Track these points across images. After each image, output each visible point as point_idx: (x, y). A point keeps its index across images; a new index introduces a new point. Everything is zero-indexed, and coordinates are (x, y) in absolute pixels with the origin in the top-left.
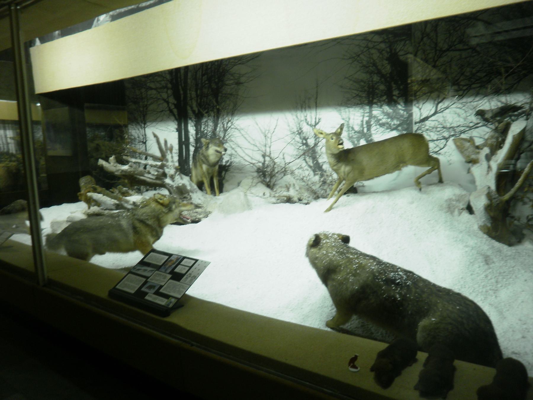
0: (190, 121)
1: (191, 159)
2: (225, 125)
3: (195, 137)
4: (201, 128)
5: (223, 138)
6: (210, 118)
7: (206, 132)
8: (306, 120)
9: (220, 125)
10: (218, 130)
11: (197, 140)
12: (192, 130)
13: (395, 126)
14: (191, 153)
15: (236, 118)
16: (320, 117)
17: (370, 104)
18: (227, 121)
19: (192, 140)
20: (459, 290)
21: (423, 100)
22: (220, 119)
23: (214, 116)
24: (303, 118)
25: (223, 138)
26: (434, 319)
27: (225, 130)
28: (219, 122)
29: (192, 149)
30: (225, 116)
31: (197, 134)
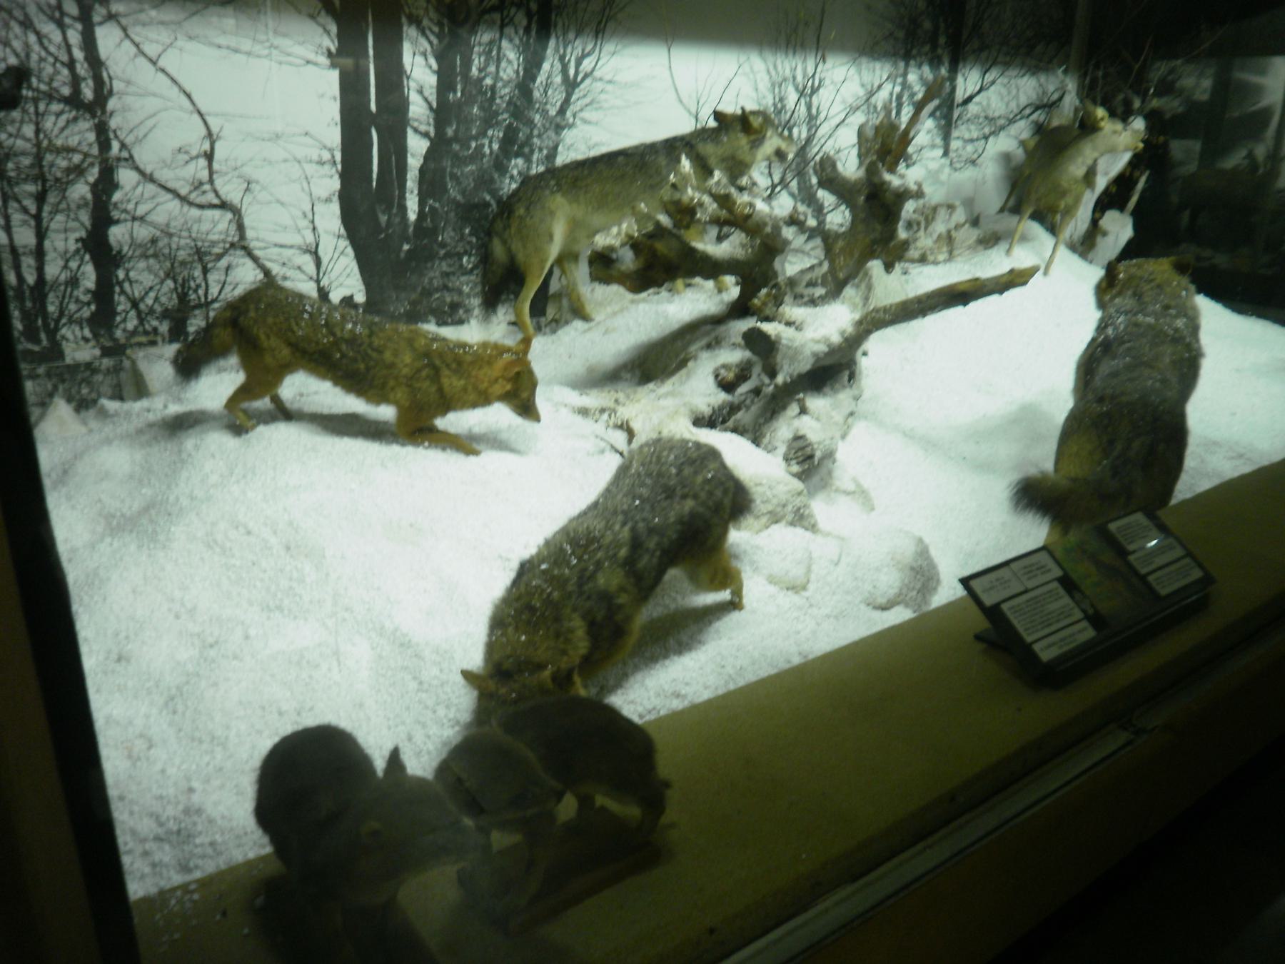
0: (410, 32)
1: (412, 182)
2: (572, 64)
3: (433, 99)
4: (467, 64)
5: (562, 111)
6: (509, 30)
7: (488, 81)
8: (794, 78)
9: (550, 66)
10: (541, 79)
11: (442, 112)
12: (420, 68)
13: (955, 116)
14: (414, 163)
15: (609, 47)
16: (823, 75)
17: (907, 57)
18: (579, 51)
19: (418, 109)
20: (121, 798)
21: (1022, 65)
22: (552, 43)
23: (527, 30)
24: (788, 72)
25: (562, 111)
26: (1154, 542)
27: (571, 85)
28: (549, 51)
29: (417, 146)
30: (571, 35)
31: (445, 85)
